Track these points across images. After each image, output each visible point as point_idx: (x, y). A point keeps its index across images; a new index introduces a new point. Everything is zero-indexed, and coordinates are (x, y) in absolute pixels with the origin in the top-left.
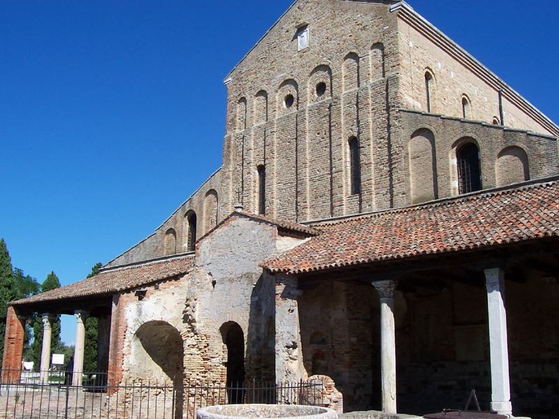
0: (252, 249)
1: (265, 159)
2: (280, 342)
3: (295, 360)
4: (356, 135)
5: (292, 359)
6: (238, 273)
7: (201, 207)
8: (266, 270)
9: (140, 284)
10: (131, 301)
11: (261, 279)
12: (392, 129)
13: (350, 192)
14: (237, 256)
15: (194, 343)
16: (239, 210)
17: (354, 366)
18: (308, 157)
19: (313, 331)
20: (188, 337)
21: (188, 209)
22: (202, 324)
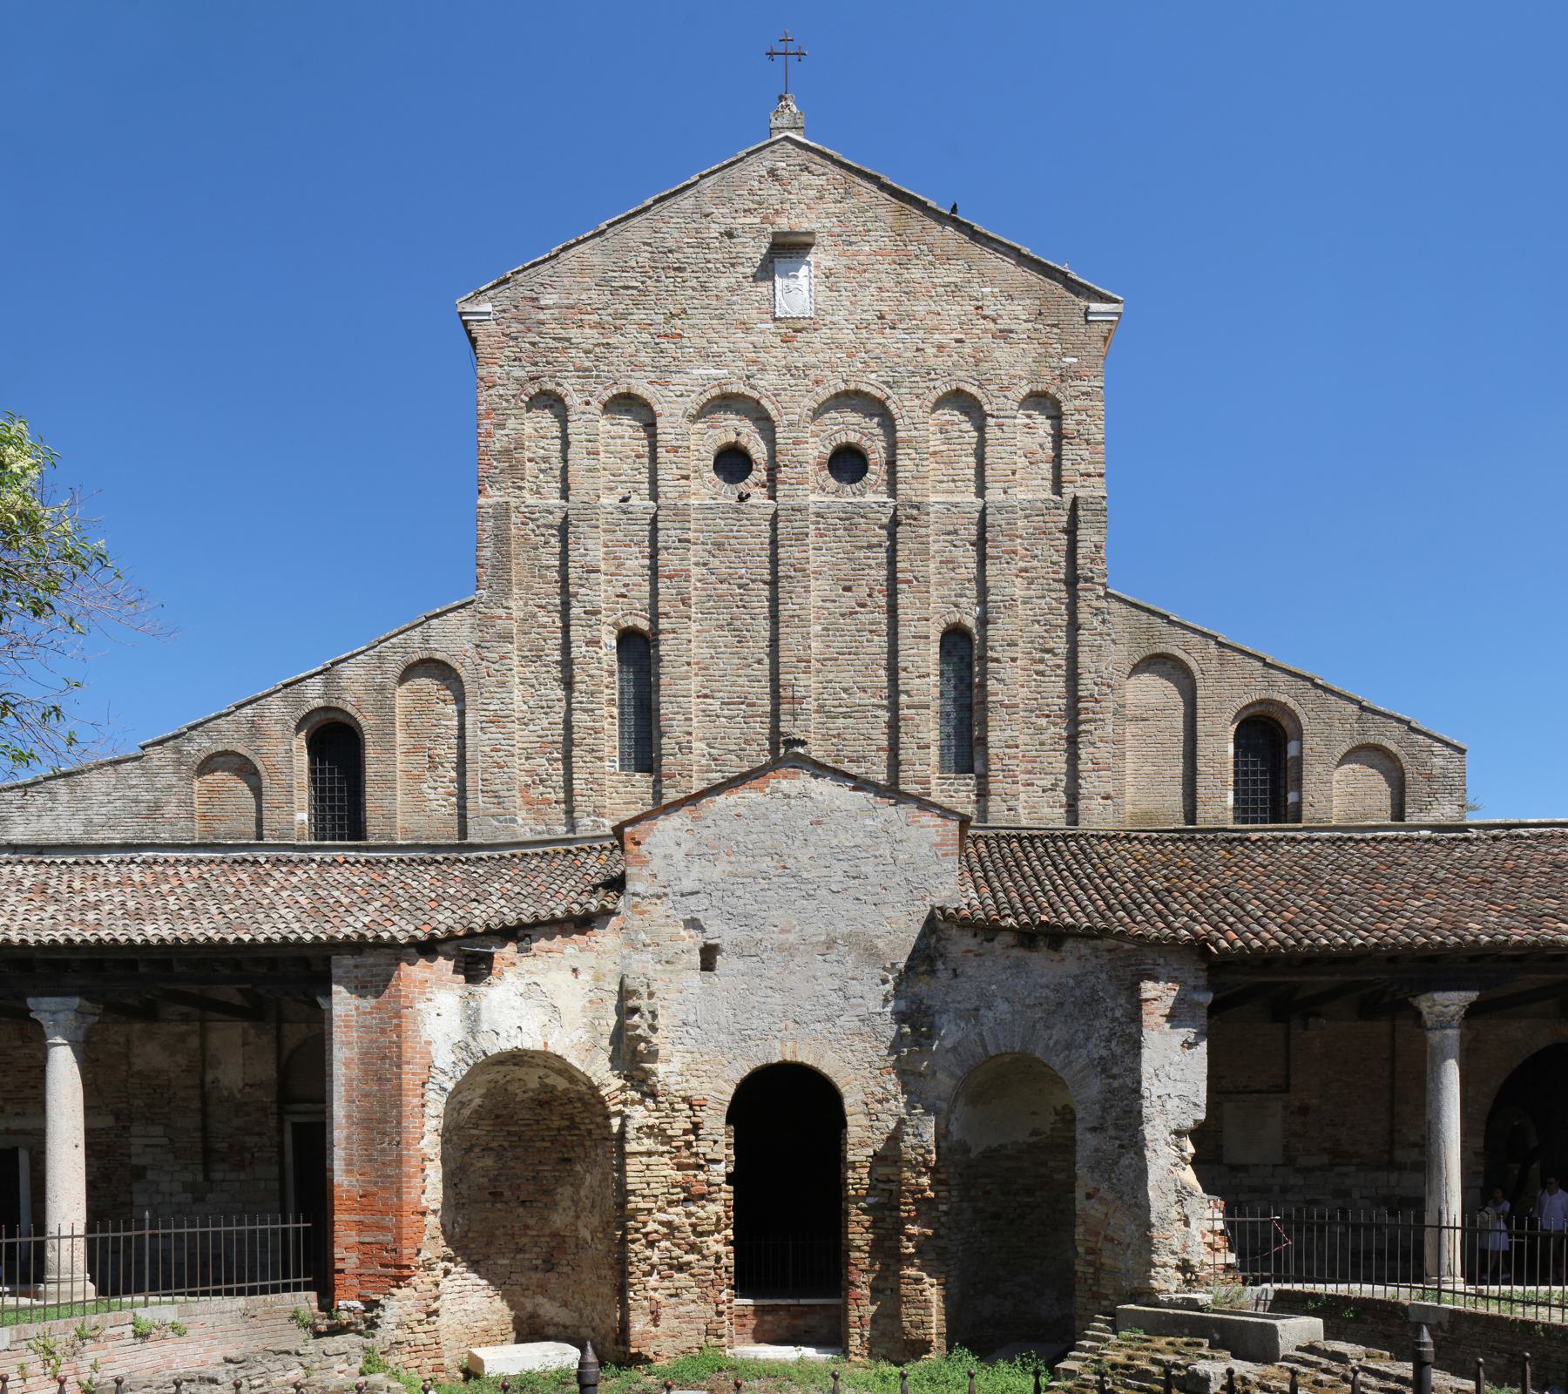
1: (655, 617)
4: (970, 622)
6: (810, 930)
12: (1084, 636)
14: (806, 881)
15: (651, 1121)
18: (816, 645)
20: (624, 1103)
22: (676, 1065)
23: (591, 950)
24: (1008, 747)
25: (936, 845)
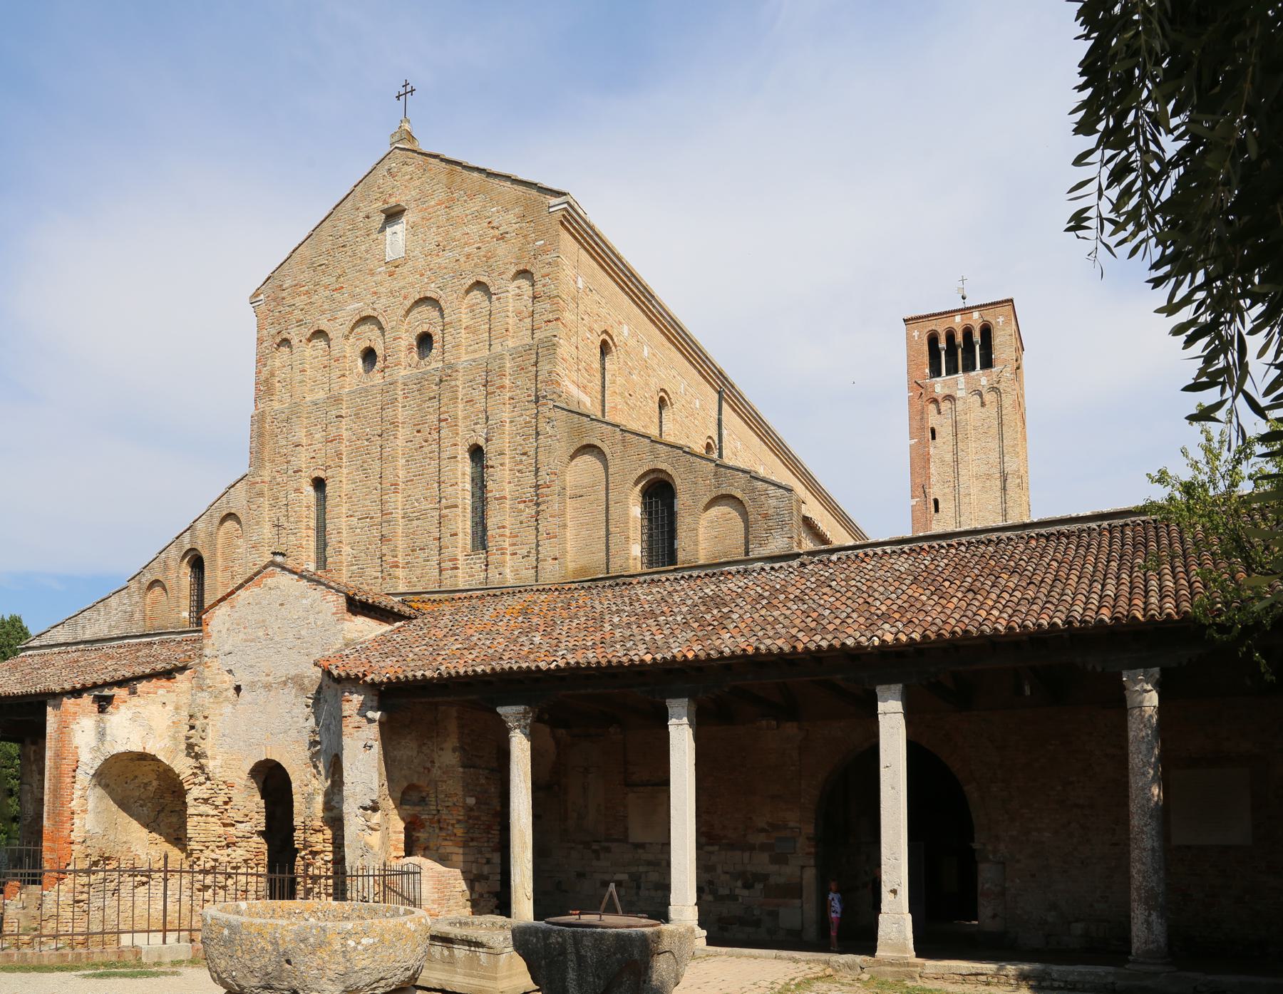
0: (303, 632)
2: (351, 800)
3: (376, 830)
5: (372, 829)
7: (213, 545)
8: (327, 673)
9: (100, 682)
10: (85, 714)
11: (320, 687)
13: (469, 547)
16: (279, 559)
17: (471, 844)
18: (401, 473)
19: (405, 784)
21: (188, 547)
23: (174, 692)
24: (499, 528)
25: (334, 614)
